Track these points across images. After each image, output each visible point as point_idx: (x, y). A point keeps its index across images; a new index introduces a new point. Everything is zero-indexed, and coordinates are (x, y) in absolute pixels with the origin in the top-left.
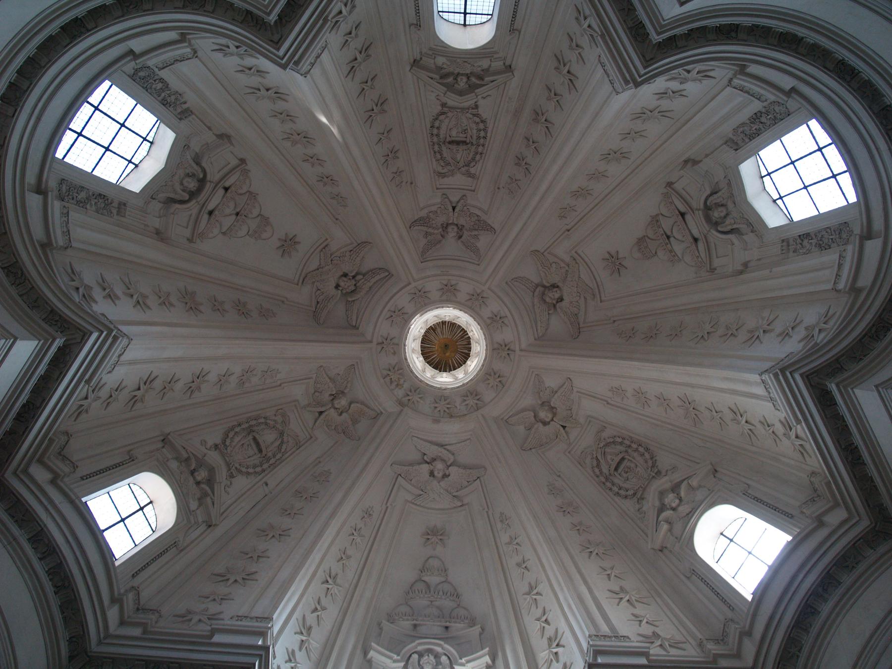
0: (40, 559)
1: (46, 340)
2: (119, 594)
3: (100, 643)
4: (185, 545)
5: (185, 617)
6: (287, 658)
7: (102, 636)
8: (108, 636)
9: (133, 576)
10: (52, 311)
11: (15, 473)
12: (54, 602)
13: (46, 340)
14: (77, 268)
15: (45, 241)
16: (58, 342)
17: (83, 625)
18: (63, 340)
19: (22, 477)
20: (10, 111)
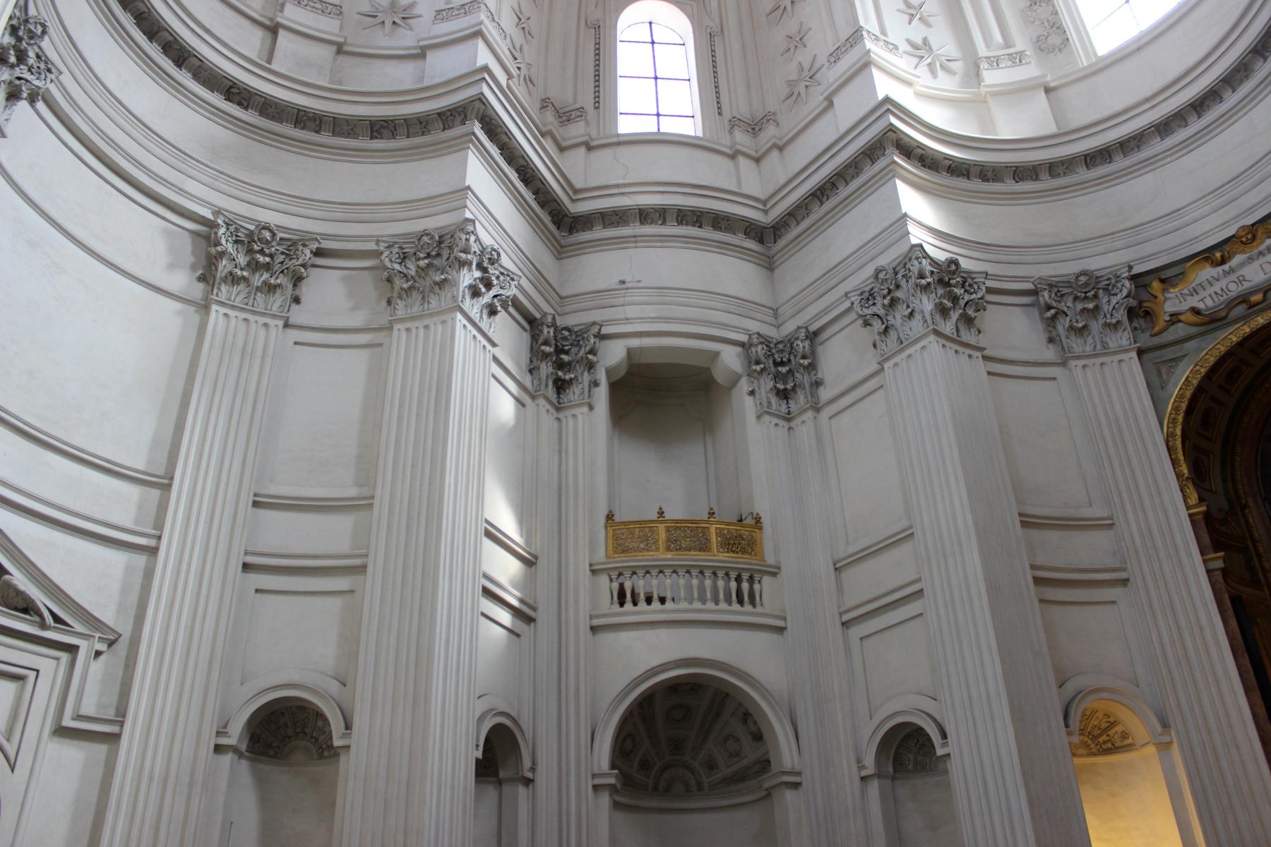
0: (664, 223)
1: (471, 141)
2: (731, 148)
3: (766, 212)
4: (717, 21)
5: (792, 96)
6: (907, 17)
7: (761, 206)
8: (765, 203)
9: (720, 114)
10: (439, 114)
11: (573, 201)
12: (707, 233)
13: (471, 141)
14: (366, 8)
15: (334, 48)
16: (477, 129)
17: (743, 219)
18: (477, 123)
19: (580, 196)
20: (193, 60)
